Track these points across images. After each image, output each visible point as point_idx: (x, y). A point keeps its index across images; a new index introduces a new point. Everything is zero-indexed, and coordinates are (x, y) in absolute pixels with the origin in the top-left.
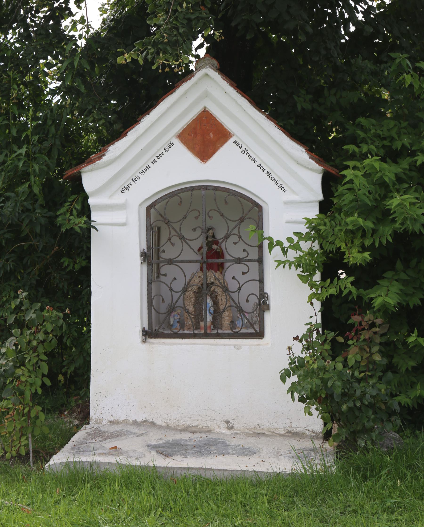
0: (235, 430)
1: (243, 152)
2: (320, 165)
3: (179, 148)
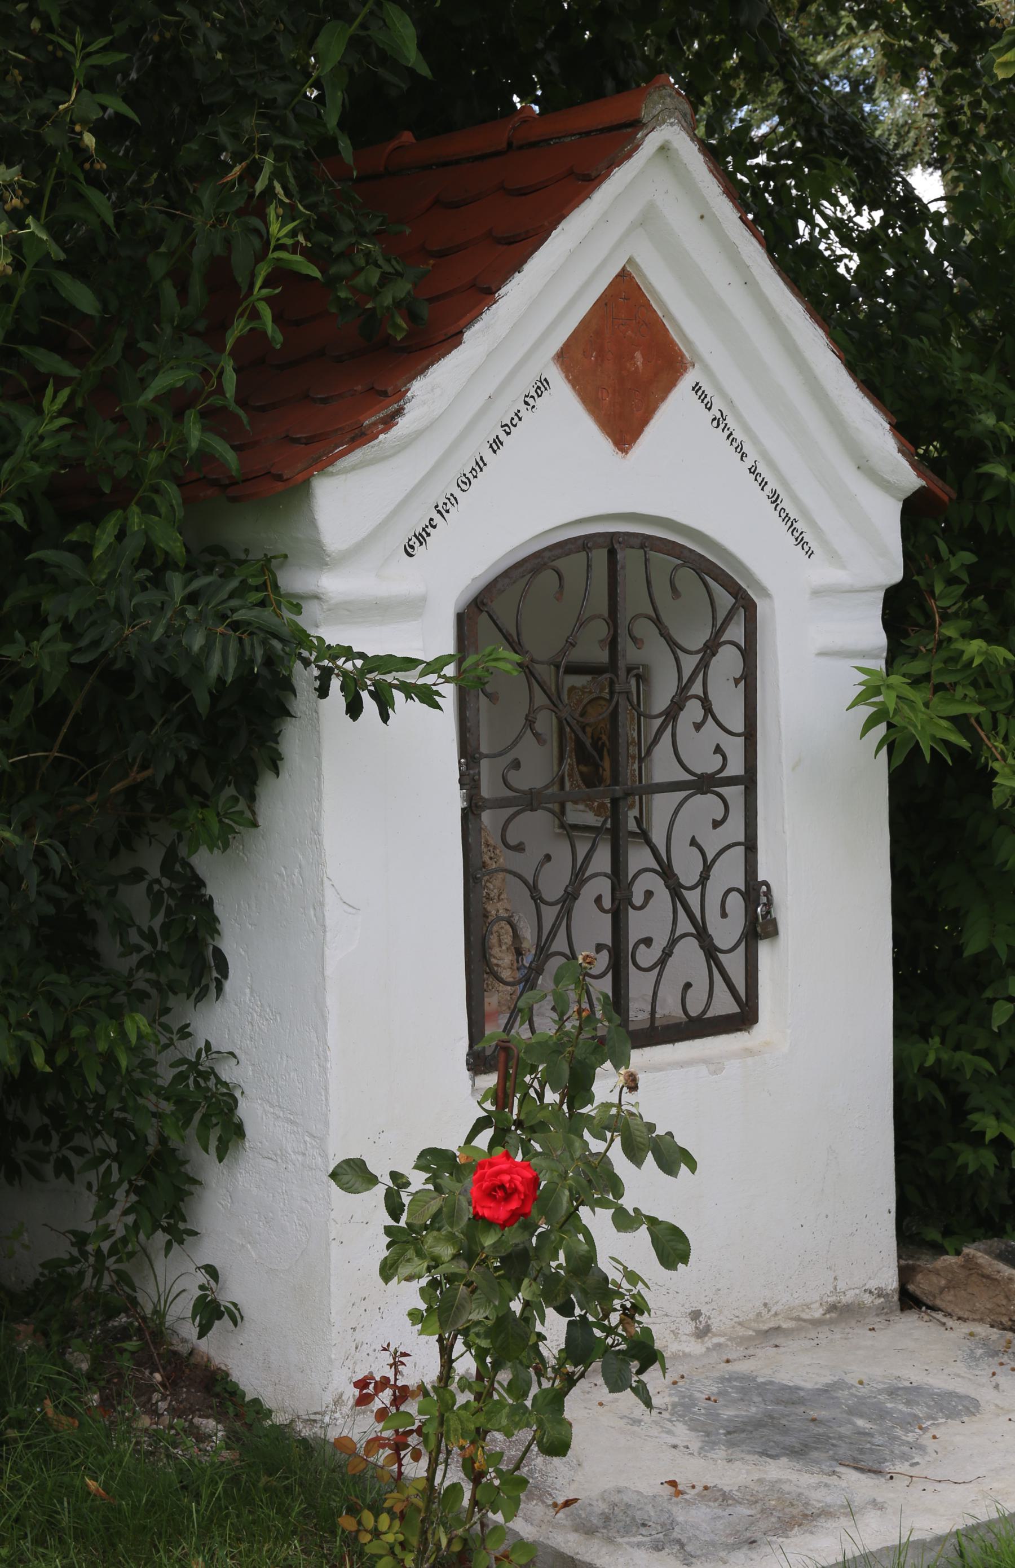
0: (715, 1335)
1: (715, 423)
2: (918, 476)
3: (563, 398)
